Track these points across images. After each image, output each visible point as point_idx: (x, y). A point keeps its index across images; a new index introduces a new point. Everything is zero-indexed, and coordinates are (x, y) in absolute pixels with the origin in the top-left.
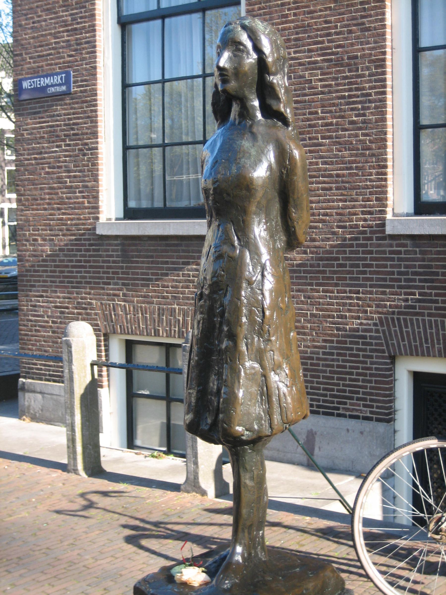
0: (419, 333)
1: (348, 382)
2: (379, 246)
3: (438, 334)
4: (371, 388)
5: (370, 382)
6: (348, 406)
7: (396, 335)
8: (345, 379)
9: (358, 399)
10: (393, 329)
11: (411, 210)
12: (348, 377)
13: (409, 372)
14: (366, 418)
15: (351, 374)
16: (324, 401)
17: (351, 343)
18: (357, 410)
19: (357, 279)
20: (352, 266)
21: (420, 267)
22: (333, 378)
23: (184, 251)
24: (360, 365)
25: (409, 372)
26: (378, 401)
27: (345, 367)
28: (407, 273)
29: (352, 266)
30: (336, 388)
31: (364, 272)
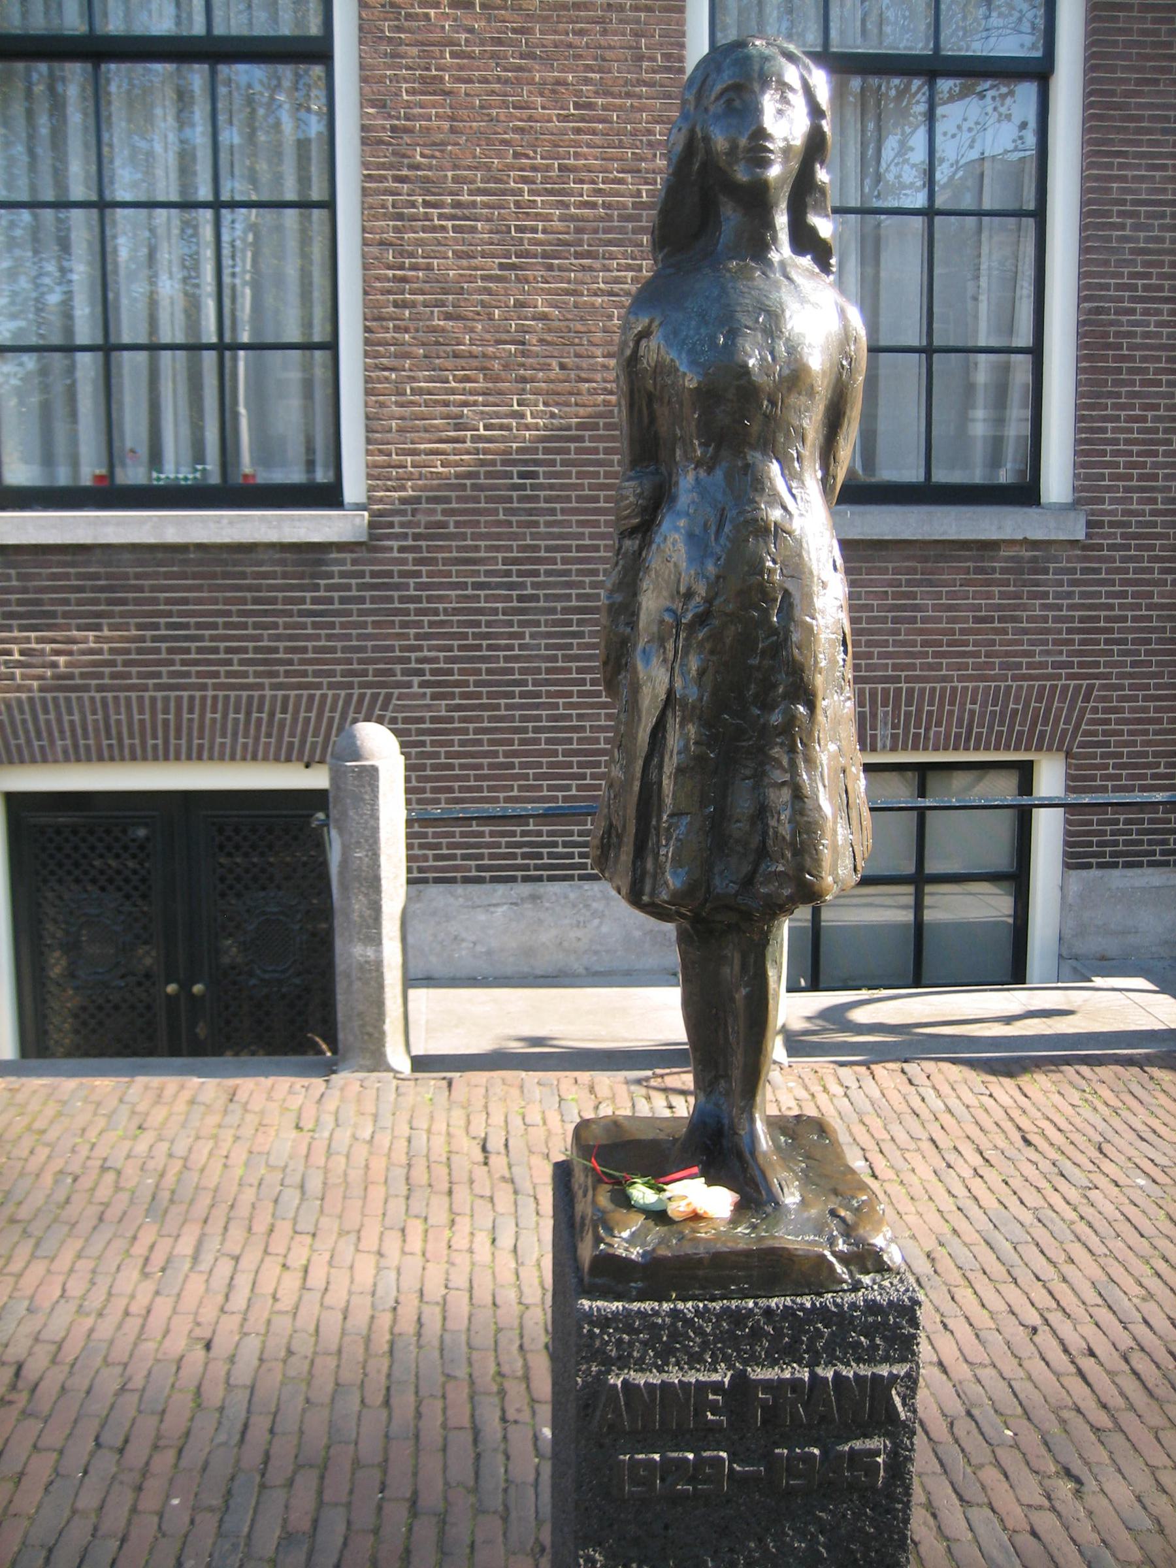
0: (24, 721)
3: (59, 720)
21: (20, 603)
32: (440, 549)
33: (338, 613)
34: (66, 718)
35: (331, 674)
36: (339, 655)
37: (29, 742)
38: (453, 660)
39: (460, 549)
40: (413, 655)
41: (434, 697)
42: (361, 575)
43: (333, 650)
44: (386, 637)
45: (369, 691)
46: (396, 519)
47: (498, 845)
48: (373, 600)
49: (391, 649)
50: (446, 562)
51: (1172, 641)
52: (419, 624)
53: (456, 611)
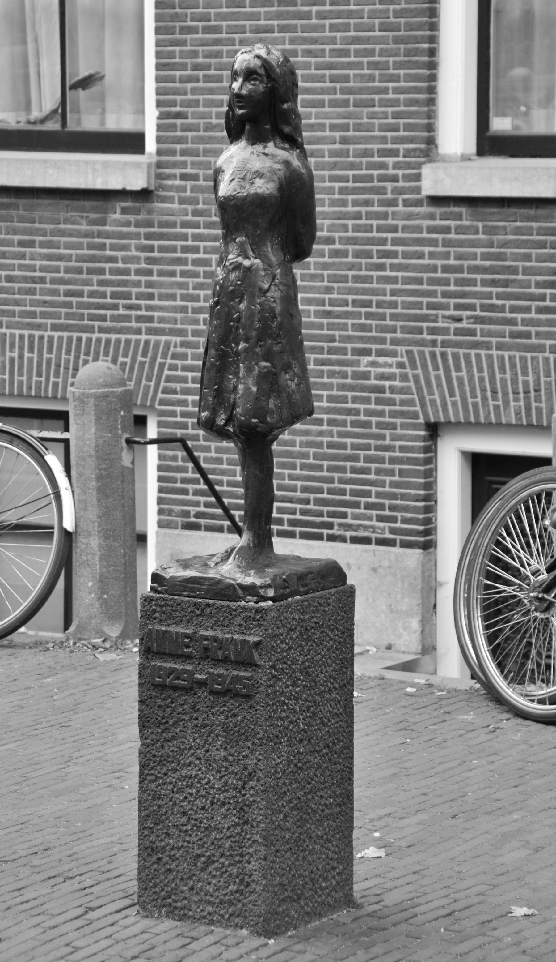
0: (482, 379)
1: (349, 475)
2: (409, 217)
3: (515, 381)
4: (393, 484)
5: (391, 473)
6: (349, 521)
7: (439, 385)
8: (343, 470)
9: (368, 506)
10: (432, 373)
11: (472, 148)
12: (349, 464)
13: (464, 454)
14: (382, 542)
15: (355, 458)
16: (304, 512)
17: (355, 400)
18: (366, 528)
19: (367, 279)
20: (357, 254)
21: (485, 256)
22: (320, 468)
23: (22, 219)
24: (372, 442)
25: (464, 454)
26: (406, 509)
27: (343, 446)
28: (459, 269)
29: (357, 254)
30: (325, 486)
31: (381, 267)
34: (521, 378)
37: (484, 399)
51: (3, 313)
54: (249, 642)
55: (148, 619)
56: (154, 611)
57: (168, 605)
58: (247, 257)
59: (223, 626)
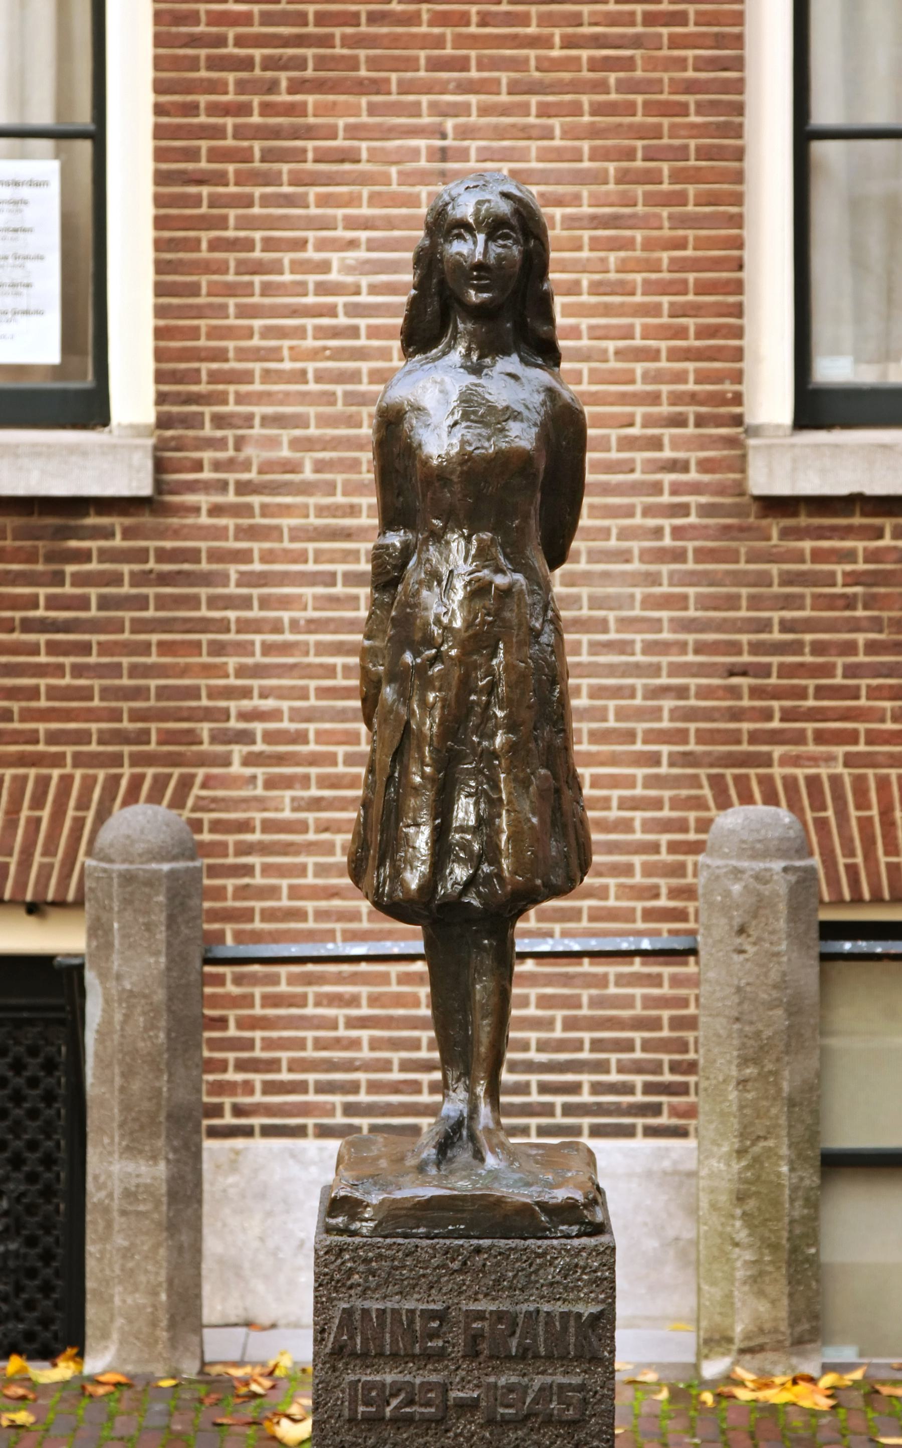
32: (286, 510)
33: (94, 626)
35: (82, 737)
36: (96, 703)
38: (309, 716)
39: (321, 511)
40: (233, 706)
41: (270, 784)
42: (141, 556)
43: (86, 694)
44: (184, 671)
45: (150, 772)
46: (207, 456)
47: (386, 1066)
48: (162, 603)
49: (193, 693)
50: (297, 534)
52: (244, 648)
53: (314, 626)
54: (579, 1315)
55: (336, 1290)
56: (351, 1272)
57: (386, 1258)
58: (499, 570)
59: (511, 1288)
